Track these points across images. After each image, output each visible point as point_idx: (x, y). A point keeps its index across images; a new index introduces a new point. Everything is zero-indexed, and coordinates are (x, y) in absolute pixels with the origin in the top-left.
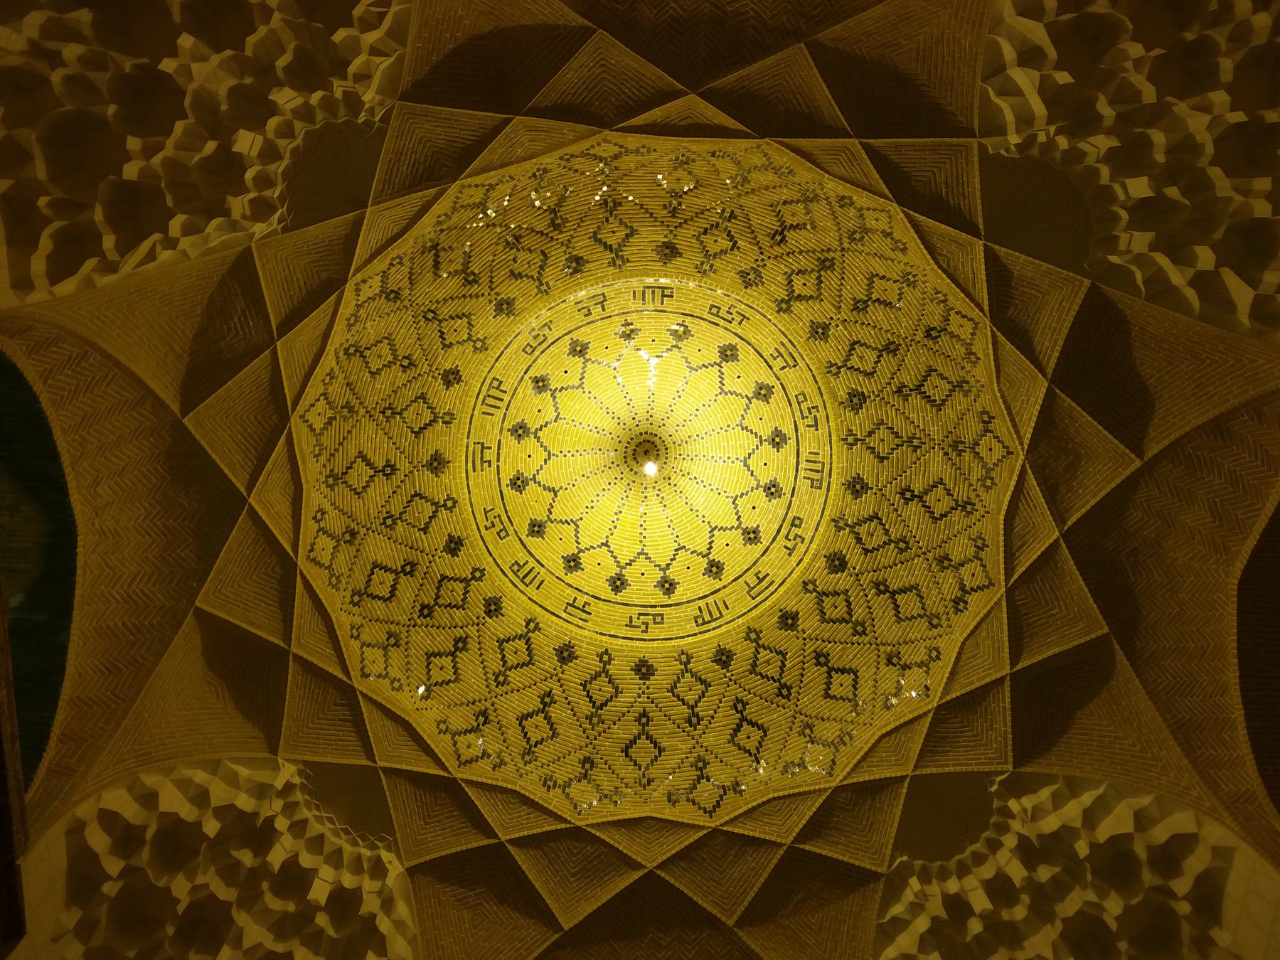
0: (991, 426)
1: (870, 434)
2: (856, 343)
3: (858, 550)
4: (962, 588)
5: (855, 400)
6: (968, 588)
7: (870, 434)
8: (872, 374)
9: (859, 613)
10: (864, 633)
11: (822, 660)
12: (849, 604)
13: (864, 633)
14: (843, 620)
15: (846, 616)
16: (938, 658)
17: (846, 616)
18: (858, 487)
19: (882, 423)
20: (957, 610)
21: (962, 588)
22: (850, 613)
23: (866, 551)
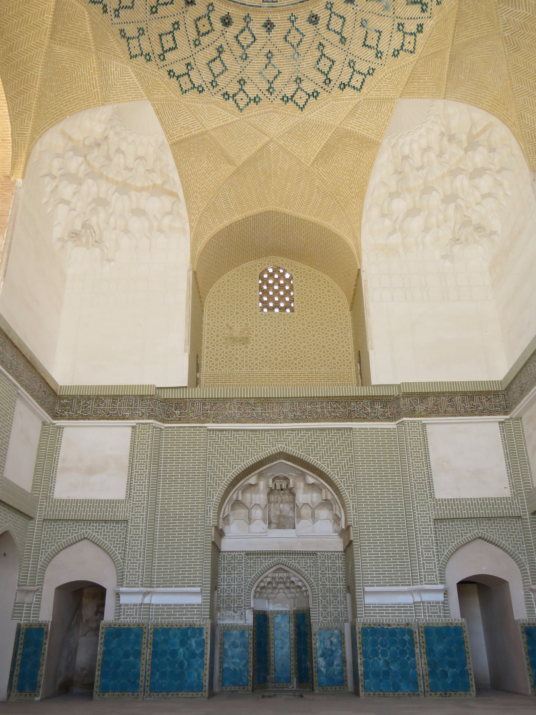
0: (312, 98)
1: (297, 29)
2: (344, 19)
3: (236, 32)
4: (234, 95)
5: (314, 19)
6: (235, 98)
7: (297, 29)
8: (328, 28)
9: (205, 40)
10: (196, 45)
11: (176, 26)
12: (207, 33)
13: (196, 45)
14: (199, 32)
15: (201, 34)
16: (200, 92)
17: (201, 34)
18: (269, 26)
19: (304, 36)
20: (224, 95)
21: (234, 95)
22: (203, 35)
23: (236, 37)
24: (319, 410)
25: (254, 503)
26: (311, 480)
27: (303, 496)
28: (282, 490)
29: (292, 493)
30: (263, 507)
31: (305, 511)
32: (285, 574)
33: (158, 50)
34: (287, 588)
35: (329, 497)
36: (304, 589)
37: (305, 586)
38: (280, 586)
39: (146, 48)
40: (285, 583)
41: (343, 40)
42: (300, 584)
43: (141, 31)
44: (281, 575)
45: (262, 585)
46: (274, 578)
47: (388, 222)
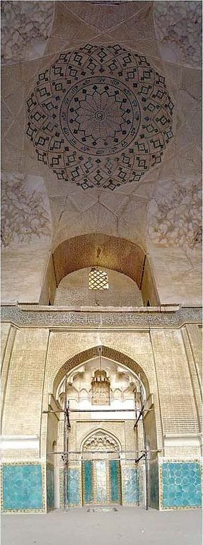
24: (127, 320)
25: (82, 388)
26: (120, 370)
27: (115, 384)
28: (101, 382)
29: (108, 384)
30: (88, 391)
31: (117, 394)
32: (104, 436)
33: (51, 162)
34: (105, 445)
35: (134, 381)
36: (116, 445)
37: (117, 443)
38: (100, 444)
39: (46, 160)
40: (103, 442)
41: (130, 166)
42: (113, 442)
43: (45, 154)
44: (100, 437)
45: (88, 443)
46: (96, 439)
47: (159, 234)
